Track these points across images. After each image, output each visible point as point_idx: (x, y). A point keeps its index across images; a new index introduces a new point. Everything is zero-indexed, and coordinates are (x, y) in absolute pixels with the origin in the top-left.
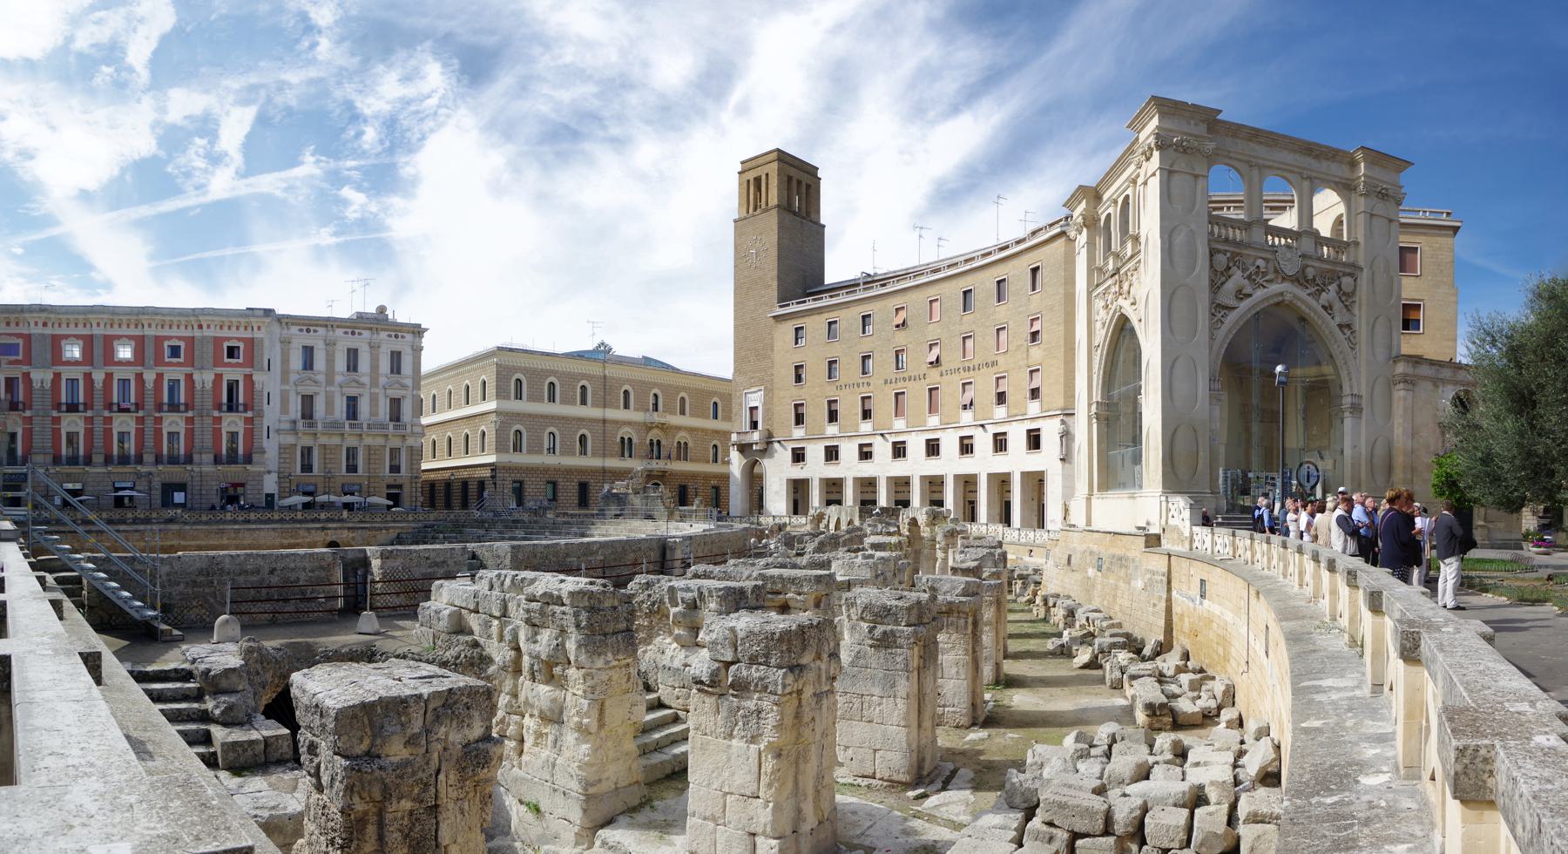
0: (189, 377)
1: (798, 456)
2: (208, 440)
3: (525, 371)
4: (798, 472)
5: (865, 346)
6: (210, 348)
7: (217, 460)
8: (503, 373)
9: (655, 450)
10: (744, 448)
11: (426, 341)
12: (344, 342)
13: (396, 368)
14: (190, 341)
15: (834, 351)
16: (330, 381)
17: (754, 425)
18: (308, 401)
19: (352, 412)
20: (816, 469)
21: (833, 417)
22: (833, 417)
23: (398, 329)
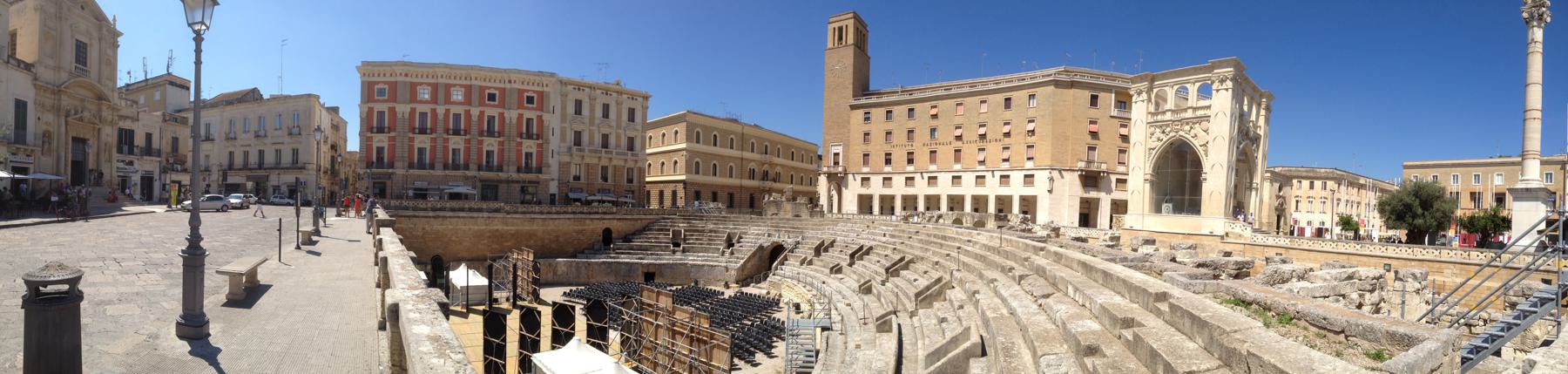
0: (502, 115)
1: (865, 180)
2: (513, 157)
3: (704, 127)
4: (864, 191)
5: (911, 124)
6: (515, 96)
7: (519, 170)
8: (690, 128)
9: (765, 176)
10: (831, 177)
11: (650, 103)
12: (602, 99)
13: (631, 118)
14: (503, 91)
15: (890, 126)
16: (592, 123)
17: (836, 163)
18: (578, 135)
19: (605, 145)
20: (876, 188)
21: (888, 162)
22: (888, 162)
23: (633, 96)
